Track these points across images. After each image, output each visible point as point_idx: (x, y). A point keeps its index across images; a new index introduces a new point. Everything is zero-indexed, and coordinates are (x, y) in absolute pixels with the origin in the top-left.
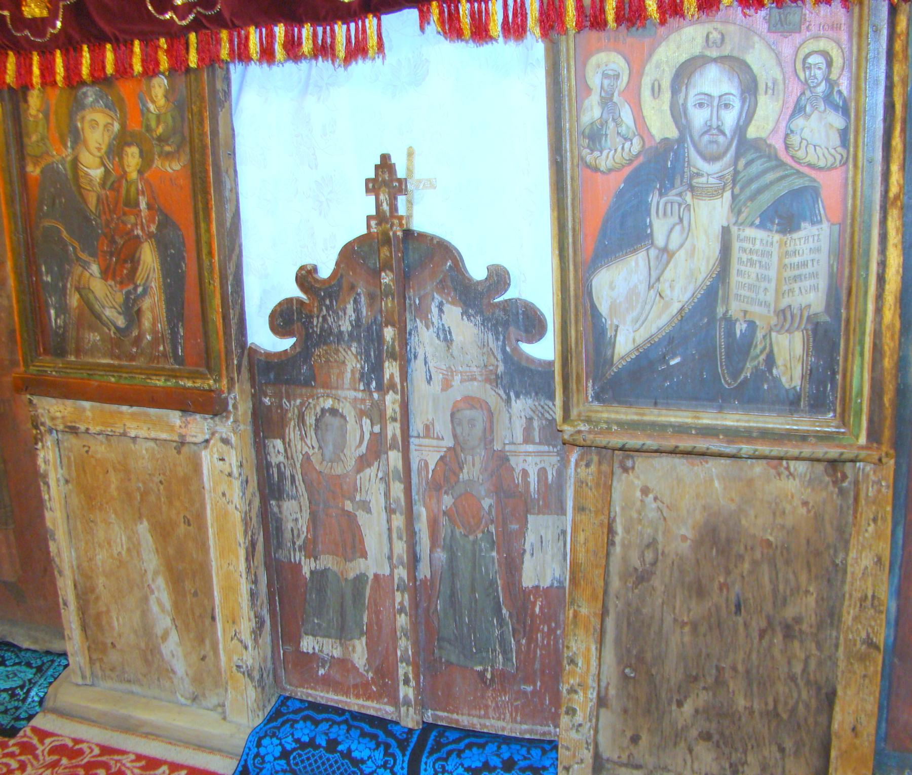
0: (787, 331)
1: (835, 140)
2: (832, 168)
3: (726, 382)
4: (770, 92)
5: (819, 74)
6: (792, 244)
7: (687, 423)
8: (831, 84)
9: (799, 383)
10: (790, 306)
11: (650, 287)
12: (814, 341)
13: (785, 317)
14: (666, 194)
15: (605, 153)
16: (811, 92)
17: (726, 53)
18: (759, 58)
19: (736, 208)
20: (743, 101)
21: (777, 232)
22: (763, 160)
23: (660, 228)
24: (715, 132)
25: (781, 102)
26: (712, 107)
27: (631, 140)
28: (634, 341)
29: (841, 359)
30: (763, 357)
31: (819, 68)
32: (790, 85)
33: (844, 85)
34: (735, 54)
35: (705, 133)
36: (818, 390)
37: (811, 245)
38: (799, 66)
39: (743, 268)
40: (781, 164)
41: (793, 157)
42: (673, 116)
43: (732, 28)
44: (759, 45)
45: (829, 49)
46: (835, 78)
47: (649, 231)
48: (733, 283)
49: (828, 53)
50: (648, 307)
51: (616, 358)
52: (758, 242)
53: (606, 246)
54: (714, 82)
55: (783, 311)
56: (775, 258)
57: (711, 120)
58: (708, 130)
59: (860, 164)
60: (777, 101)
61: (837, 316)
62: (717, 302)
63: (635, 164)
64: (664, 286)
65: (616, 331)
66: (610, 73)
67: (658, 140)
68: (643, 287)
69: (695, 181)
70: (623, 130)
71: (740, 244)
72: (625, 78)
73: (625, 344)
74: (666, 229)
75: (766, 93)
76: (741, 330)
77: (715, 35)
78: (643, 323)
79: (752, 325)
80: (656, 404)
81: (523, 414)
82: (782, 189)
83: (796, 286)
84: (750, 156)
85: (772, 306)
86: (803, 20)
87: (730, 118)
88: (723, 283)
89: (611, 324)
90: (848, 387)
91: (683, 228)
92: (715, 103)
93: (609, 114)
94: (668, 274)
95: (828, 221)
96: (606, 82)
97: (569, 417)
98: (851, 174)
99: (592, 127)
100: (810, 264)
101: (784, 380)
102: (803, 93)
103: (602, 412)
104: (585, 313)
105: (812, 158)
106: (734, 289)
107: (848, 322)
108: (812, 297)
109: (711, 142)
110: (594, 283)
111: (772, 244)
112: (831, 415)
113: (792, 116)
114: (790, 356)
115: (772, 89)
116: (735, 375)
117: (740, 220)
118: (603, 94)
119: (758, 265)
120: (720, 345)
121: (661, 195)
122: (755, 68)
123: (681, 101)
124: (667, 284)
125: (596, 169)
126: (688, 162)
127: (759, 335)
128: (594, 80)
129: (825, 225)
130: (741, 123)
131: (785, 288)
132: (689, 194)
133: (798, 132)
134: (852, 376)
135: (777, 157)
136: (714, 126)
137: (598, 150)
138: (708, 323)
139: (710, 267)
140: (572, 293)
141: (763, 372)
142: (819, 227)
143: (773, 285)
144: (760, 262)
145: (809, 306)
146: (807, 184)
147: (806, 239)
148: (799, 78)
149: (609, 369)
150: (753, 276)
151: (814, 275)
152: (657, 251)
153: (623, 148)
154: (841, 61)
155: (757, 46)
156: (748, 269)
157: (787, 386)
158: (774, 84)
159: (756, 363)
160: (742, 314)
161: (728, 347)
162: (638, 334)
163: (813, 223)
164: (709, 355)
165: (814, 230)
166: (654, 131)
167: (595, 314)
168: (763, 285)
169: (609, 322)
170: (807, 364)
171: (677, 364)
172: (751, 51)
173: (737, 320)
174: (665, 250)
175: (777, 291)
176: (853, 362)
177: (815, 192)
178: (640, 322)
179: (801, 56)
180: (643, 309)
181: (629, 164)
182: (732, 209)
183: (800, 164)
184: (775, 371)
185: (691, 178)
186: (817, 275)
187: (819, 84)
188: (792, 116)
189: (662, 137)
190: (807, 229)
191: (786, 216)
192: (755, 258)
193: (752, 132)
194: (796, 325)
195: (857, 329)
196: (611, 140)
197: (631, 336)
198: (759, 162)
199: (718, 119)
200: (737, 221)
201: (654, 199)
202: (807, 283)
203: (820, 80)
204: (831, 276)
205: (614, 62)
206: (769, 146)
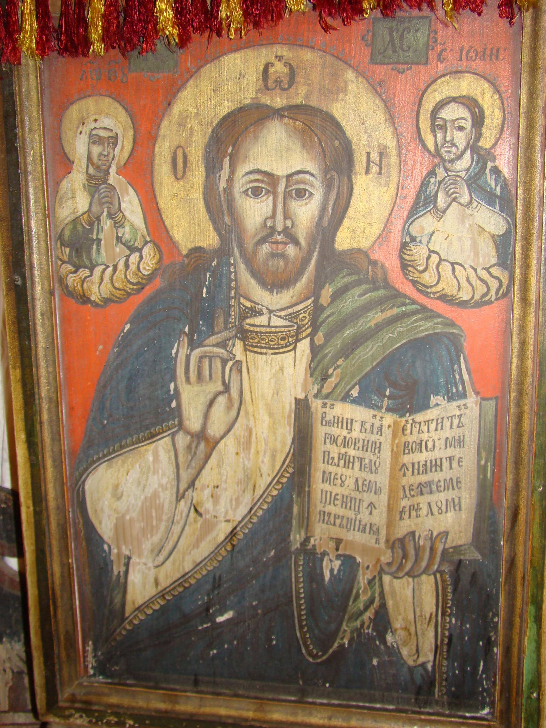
0: (408, 574)
1: (489, 254)
2: (479, 304)
3: (310, 654)
4: (374, 169)
5: (461, 139)
6: (415, 430)
7: (246, 720)
8: (482, 157)
9: (431, 658)
10: (413, 533)
11: (180, 497)
12: (455, 590)
13: (405, 552)
14: (201, 345)
15: (98, 270)
16: (446, 170)
17: (298, 101)
19: (318, 370)
20: (328, 186)
21: (388, 410)
22: (364, 287)
23: (192, 401)
24: (280, 238)
25: (393, 187)
26: (275, 193)
27: (140, 250)
28: (157, 582)
29: (500, 620)
30: (369, 614)
31: (461, 129)
32: (409, 157)
33: (504, 160)
34: (314, 102)
35: (263, 241)
36: (462, 669)
37: (447, 433)
38: (425, 123)
39: (332, 469)
40: (396, 296)
41: (414, 283)
42: (209, 210)
43: (307, 55)
44: (354, 85)
45: (476, 93)
46: (488, 146)
47: (174, 404)
48: (317, 495)
49: (475, 101)
50: (176, 529)
51: (129, 609)
52: (357, 426)
53: (104, 426)
54: (277, 151)
55: (402, 541)
56: (386, 455)
57: (273, 216)
58: (268, 233)
59: (533, 297)
60: (387, 185)
61: (493, 551)
62: (290, 523)
63: (148, 291)
64: (202, 495)
65: (127, 565)
66: (104, 134)
67: (184, 252)
68: (167, 497)
69: (248, 321)
70: (126, 233)
71: (327, 429)
72: (128, 146)
73: (142, 584)
74: (203, 400)
75: (367, 171)
76: (332, 570)
77: (279, 68)
78: (170, 554)
79: (350, 563)
80: (196, 683)
81: (8, 665)
82: (397, 337)
83: (423, 501)
84: (340, 282)
85: (383, 532)
86: (432, 40)
87: (306, 213)
88: (299, 495)
89: (119, 555)
90: (514, 672)
91: (230, 399)
92: (281, 189)
93: (101, 204)
94: (208, 476)
95: (477, 393)
96: (96, 150)
97: (57, 701)
98: (517, 313)
99: (75, 227)
100: (446, 464)
101: (405, 652)
102: (432, 173)
103: (108, 695)
104: (77, 534)
105: (447, 285)
106: (318, 505)
107: (512, 563)
108: (449, 518)
109: (273, 255)
110: (87, 487)
111: (381, 428)
112: (486, 711)
113: (413, 213)
114: (414, 607)
115: (378, 163)
116: (325, 642)
117: (325, 391)
118: (91, 171)
119: (357, 465)
120: (298, 593)
121: (192, 345)
122: (350, 128)
123: (223, 185)
124: (207, 492)
125: (85, 299)
126: (237, 289)
127: (363, 579)
128: (79, 147)
129: (472, 400)
130: (325, 223)
131: (404, 503)
132: (239, 345)
133: (425, 240)
134: (521, 651)
135: (387, 285)
136: (280, 228)
137: (85, 267)
138: (278, 558)
139: (278, 468)
140: (52, 504)
141: (371, 639)
142: (461, 402)
143: (384, 498)
144: (361, 460)
145: (447, 533)
146: (440, 329)
147: (440, 423)
148: (424, 146)
149: (119, 626)
150: (350, 482)
151: (453, 484)
152: (189, 437)
153: (127, 265)
154: (498, 114)
155: (351, 87)
156: (340, 470)
157: (411, 663)
158: (381, 155)
159: (358, 623)
160: (332, 544)
161: (311, 600)
162: (163, 569)
163: (451, 398)
165: (453, 408)
166: (178, 235)
167: (91, 536)
168: (368, 497)
169: (115, 551)
170: (443, 628)
171: (228, 620)
172: (341, 96)
173: (324, 554)
174: (201, 436)
175: (390, 508)
176: (521, 635)
177: (452, 343)
178: (165, 553)
179: (428, 105)
180: (169, 531)
181: (138, 291)
182: (312, 370)
183: (427, 294)
184: (389, 638)
185: (243, 317)
186: (458, 482)
187: (460, 157)
188: (413, 213)
189: (191, 245)
190: (440, 407)
191: (403, 385)
192: (352, 452)
193: (344, 240)
194: (424, 564)
195: (528, 577)
196: (108, 251)
197: (152, 573)
198: (357, 291)
199: (287, 215)
200: (319, 391)
201: (180, 350)
202: (442, 497)
203: (461, 147)
204: (483, 486)
205: (108, 115)
206: (375, 263)
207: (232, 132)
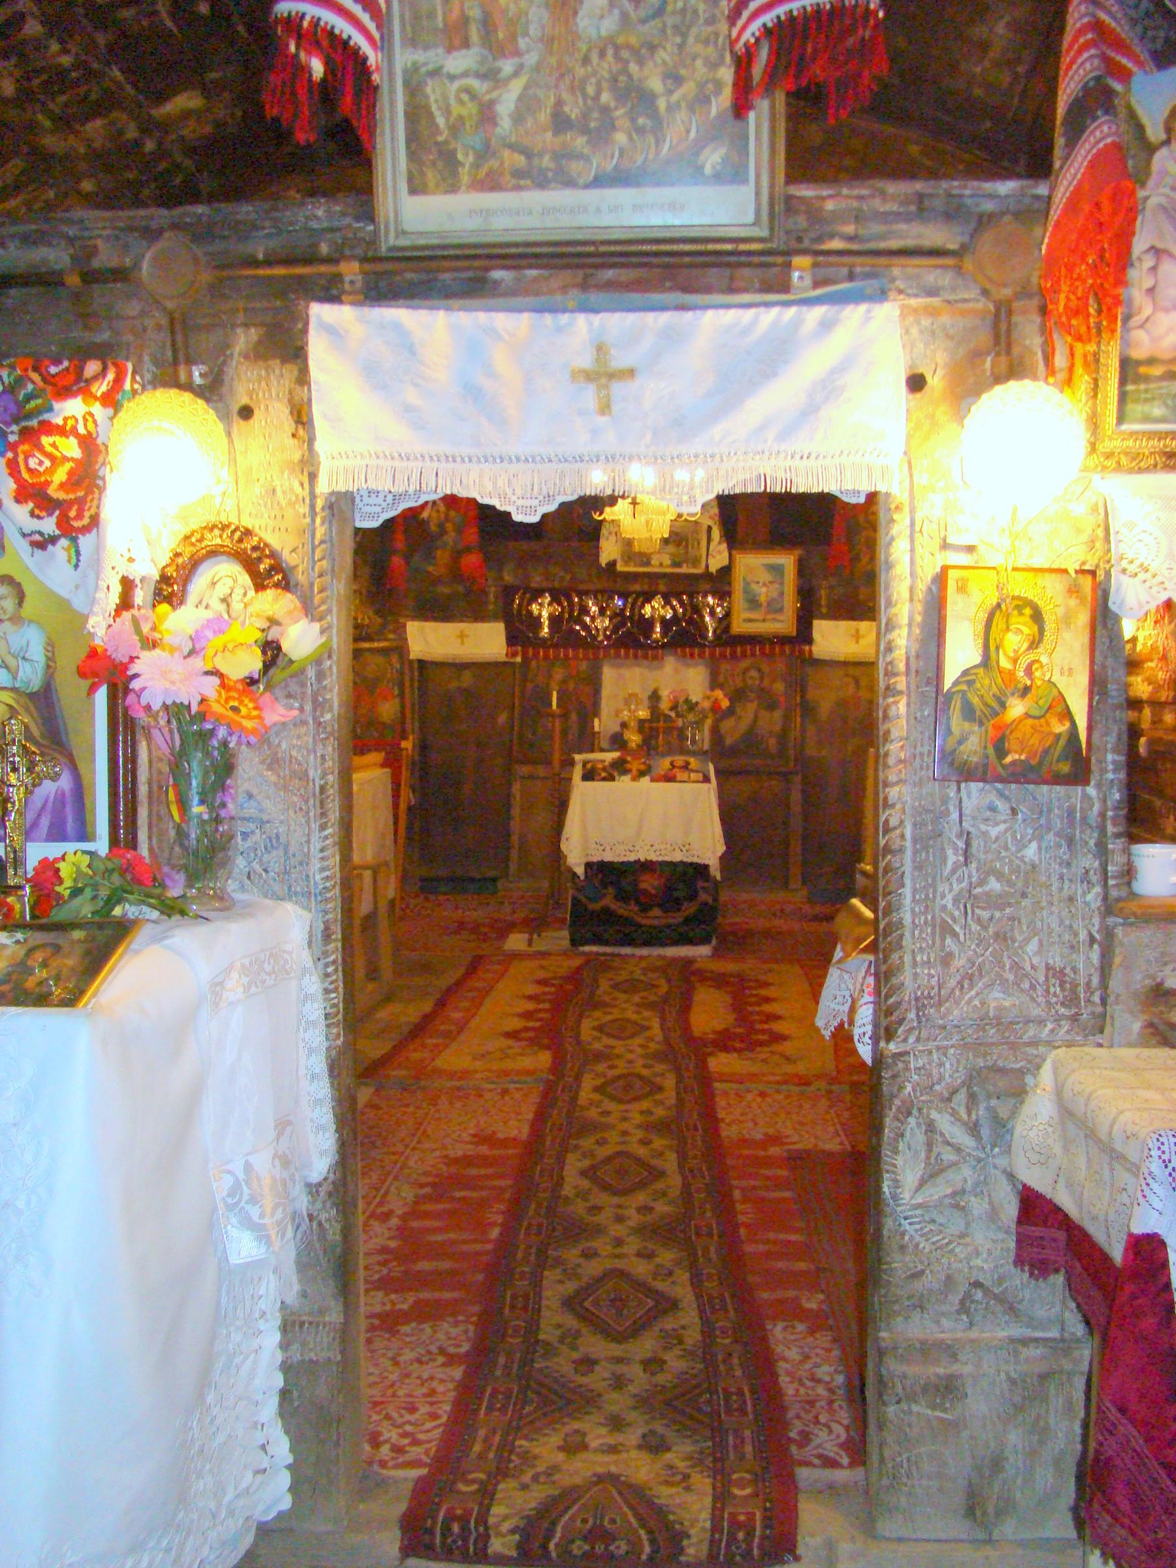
18: (765, 668)
73: (728, 741)
108: (778, 728)
191: (771, 707)
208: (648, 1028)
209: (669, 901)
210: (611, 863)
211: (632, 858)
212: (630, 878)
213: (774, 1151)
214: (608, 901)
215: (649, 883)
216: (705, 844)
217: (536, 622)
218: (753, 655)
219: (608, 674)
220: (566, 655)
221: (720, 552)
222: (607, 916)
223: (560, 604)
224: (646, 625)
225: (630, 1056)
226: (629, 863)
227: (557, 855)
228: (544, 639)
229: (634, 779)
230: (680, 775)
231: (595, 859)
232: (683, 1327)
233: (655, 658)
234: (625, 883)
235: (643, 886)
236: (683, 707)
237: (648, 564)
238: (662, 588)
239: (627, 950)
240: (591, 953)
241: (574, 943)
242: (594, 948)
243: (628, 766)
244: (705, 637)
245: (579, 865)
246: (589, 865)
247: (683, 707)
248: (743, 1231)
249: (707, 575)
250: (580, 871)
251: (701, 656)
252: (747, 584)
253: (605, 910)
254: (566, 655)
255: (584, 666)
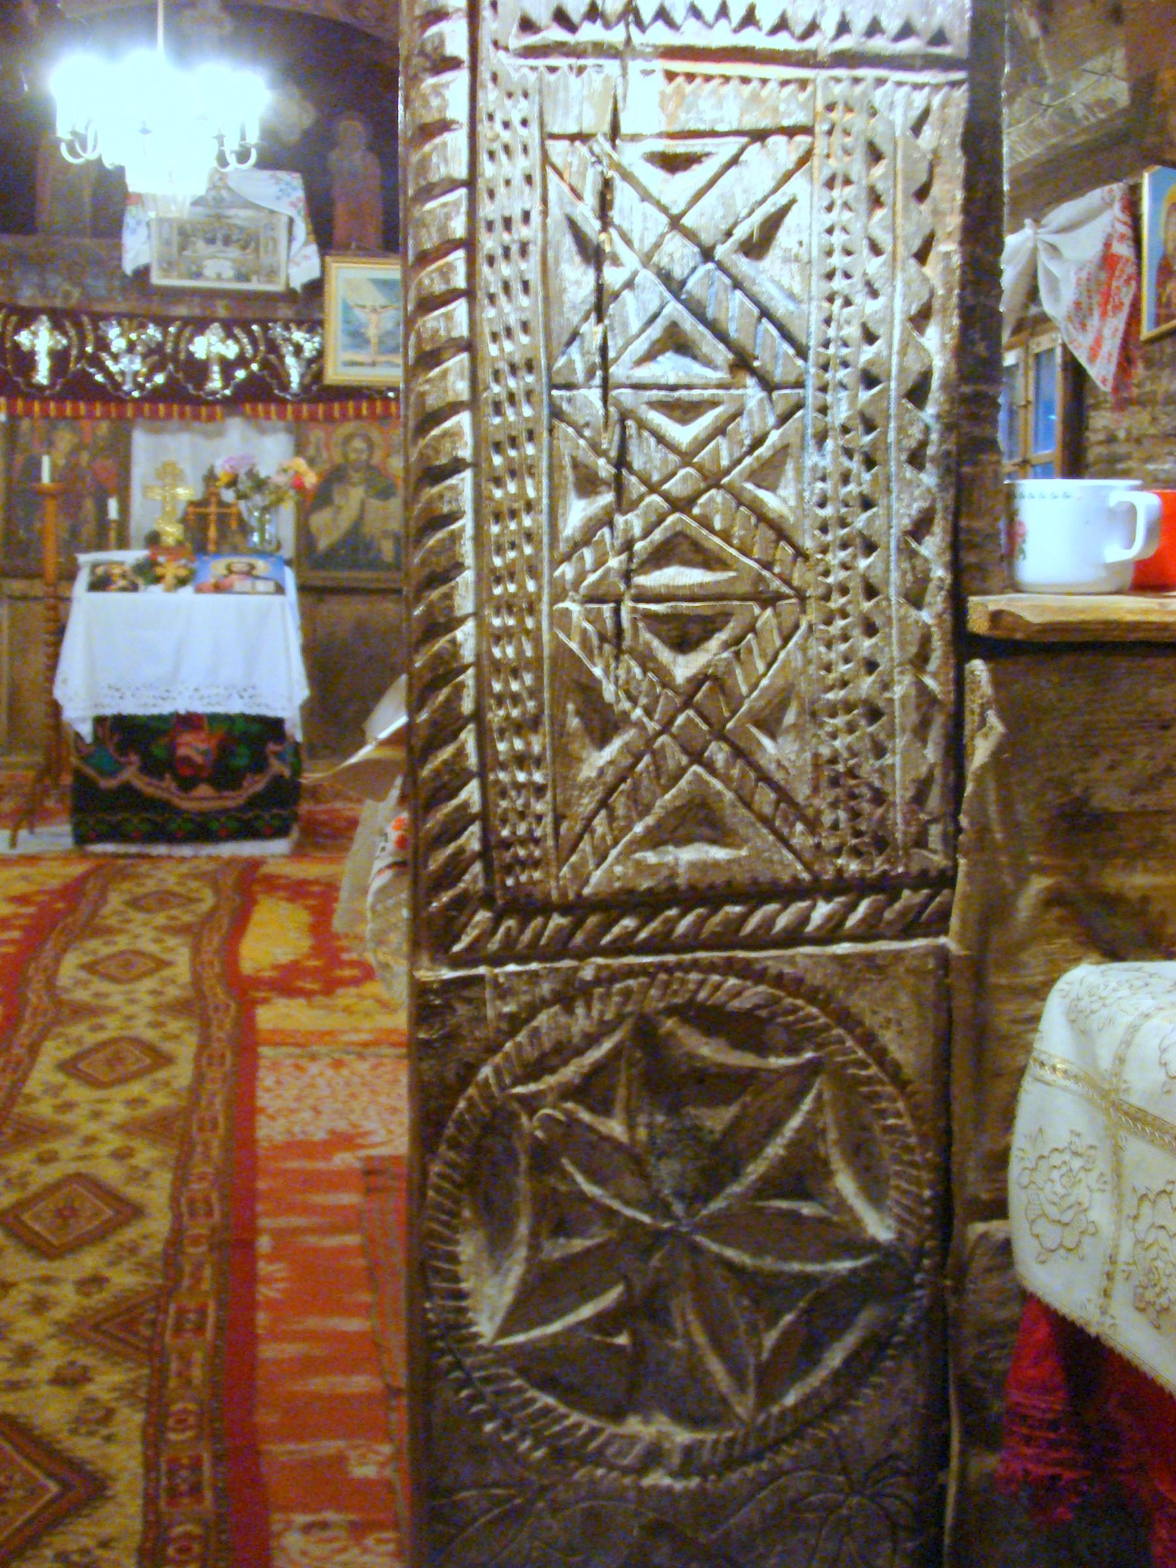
13: (386, 534)
18: (376, 435)
54: (358, 444)
73: (323, 544)
87: (364, 457)
164: (355, 550)
191: (385, 494)
207: (348, 439)
208: (168, 964)
209: (223, 775)
210: (133, 718)
211: (166, 709)
212: (164, 741)
213: (344, 1160)
214: (131, 774)
215: (193, 747)
216: (280, 688)
217: (27, 360)
218: (358, 415)
219: (142, 442)
220: (76, 409)
221: (306, 257)
222: (128, 796)
223: (65, 333)
224: (198, 370)
225: (129, 1009)
226: (161, 718)
227: (55, 709)
228: (40, 388)
229: (168, 590)
230: (239, 583)
231: (109, 711)
232: (105, 1544)
233: (211, 418)
234: (158, 751)
235: (182, 751)
236: (245, 484)
237: (198, 275)
238: (222, 312)
239: (161, 849)
240: (105, 855)
241: (81, 839)
242: (110, 848)
243: (159, 571)
244: (285, 386)
245: (83, 720)
246: (99, 721)
247: (245, 484)
248: (262, 1318)
249: (290, 296)
250: (86, 730)
251: (282, 415)
252: (347, 308)
253: (127, 788)
254: (76, 409)
255: (104, 428)
